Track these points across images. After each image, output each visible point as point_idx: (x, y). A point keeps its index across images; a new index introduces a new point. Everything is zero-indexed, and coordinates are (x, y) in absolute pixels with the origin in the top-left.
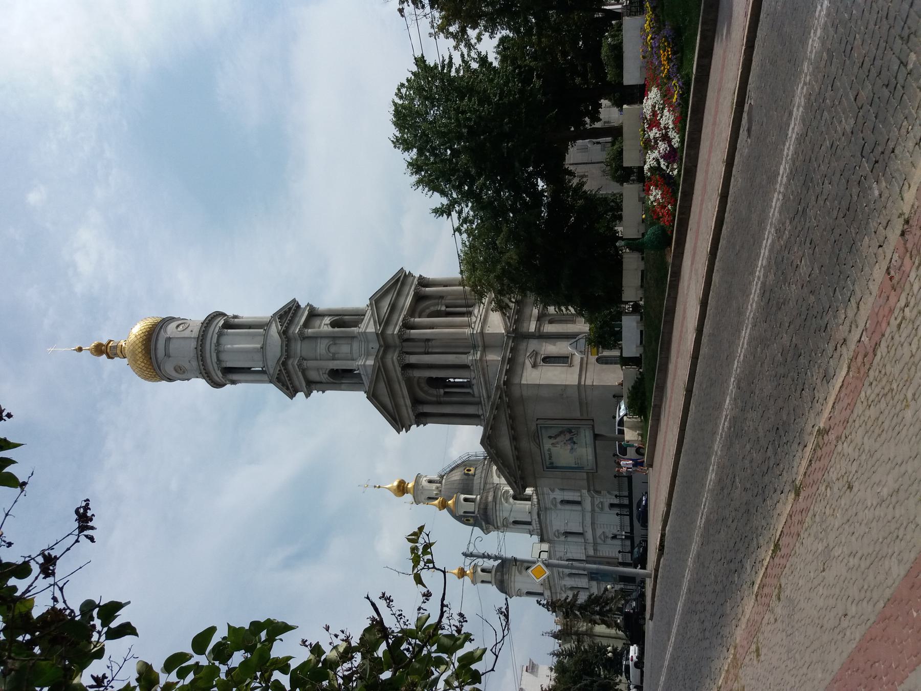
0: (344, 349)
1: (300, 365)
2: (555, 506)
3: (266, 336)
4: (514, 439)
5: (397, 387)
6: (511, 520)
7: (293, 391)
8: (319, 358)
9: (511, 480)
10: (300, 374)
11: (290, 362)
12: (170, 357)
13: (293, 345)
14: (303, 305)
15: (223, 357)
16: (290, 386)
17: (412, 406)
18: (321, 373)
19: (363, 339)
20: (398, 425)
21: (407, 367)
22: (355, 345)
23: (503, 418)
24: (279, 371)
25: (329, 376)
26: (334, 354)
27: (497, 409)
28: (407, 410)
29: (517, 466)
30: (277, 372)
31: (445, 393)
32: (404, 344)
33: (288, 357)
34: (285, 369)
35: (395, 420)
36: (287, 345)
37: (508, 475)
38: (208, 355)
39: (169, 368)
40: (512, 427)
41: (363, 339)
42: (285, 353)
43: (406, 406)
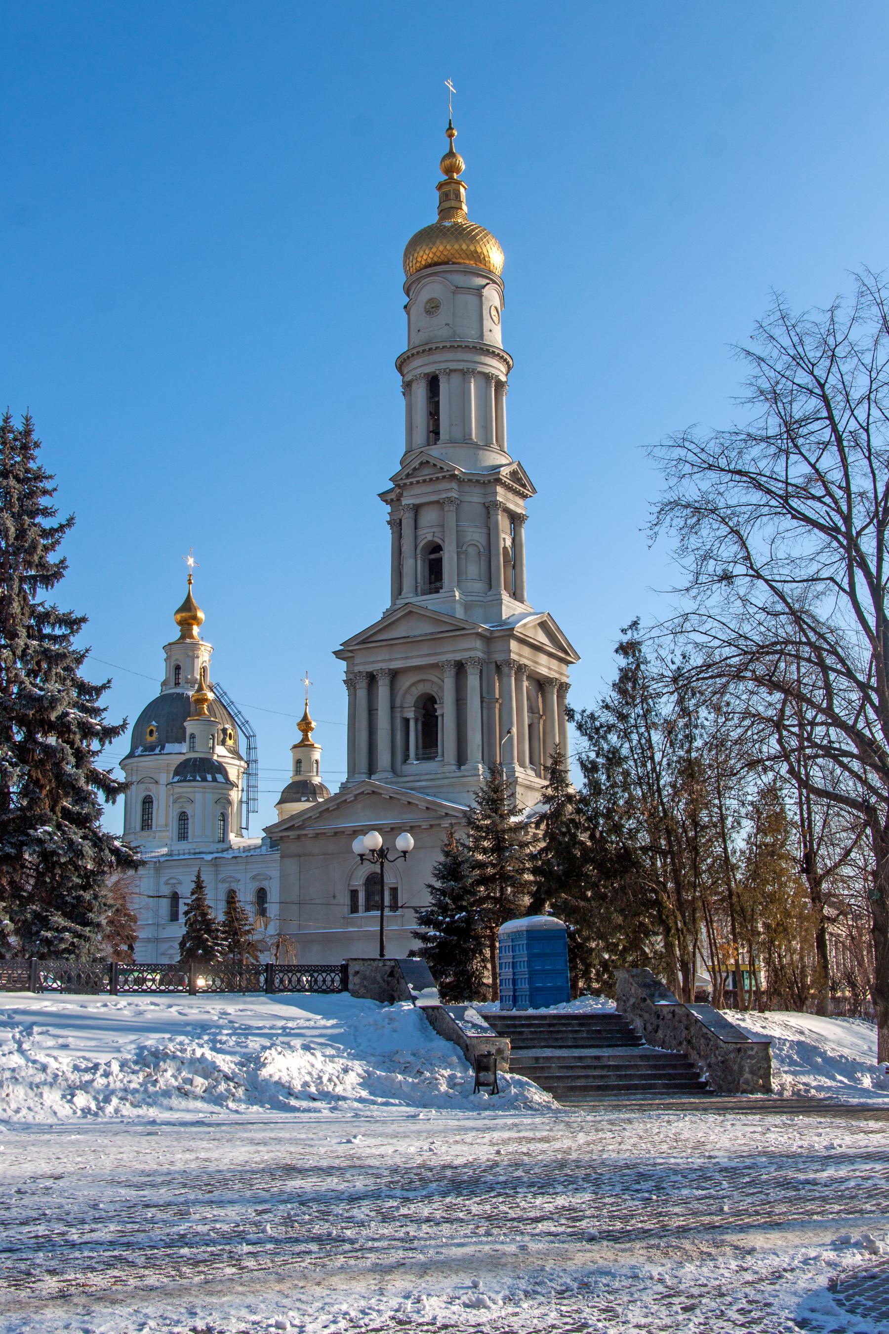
0: (473, 570)
1: (450, 500)
2: (224, 881)
5: (425, 649)
6: (189, 810)
7: (405, 484)
8: (460, 529)
9: (296, 821)
10: (435, 498)
11: (454, 485)
12: (454, 293)
13: (478, 490)
15: (456, 379)
16: (414, 480)
17: (390, 670)
21: (460, 668)
22: (479, 586)
24: (442, 468)
25: (429, 541)
26: (466, 553)
30: (439, 465)
31: (407, 721)
32: (493, 666)
34: (444, 477)
35: (364, 642)
36: (478, 481)
37: (306, 817)
39: (433, 289)
43: (391, 660)
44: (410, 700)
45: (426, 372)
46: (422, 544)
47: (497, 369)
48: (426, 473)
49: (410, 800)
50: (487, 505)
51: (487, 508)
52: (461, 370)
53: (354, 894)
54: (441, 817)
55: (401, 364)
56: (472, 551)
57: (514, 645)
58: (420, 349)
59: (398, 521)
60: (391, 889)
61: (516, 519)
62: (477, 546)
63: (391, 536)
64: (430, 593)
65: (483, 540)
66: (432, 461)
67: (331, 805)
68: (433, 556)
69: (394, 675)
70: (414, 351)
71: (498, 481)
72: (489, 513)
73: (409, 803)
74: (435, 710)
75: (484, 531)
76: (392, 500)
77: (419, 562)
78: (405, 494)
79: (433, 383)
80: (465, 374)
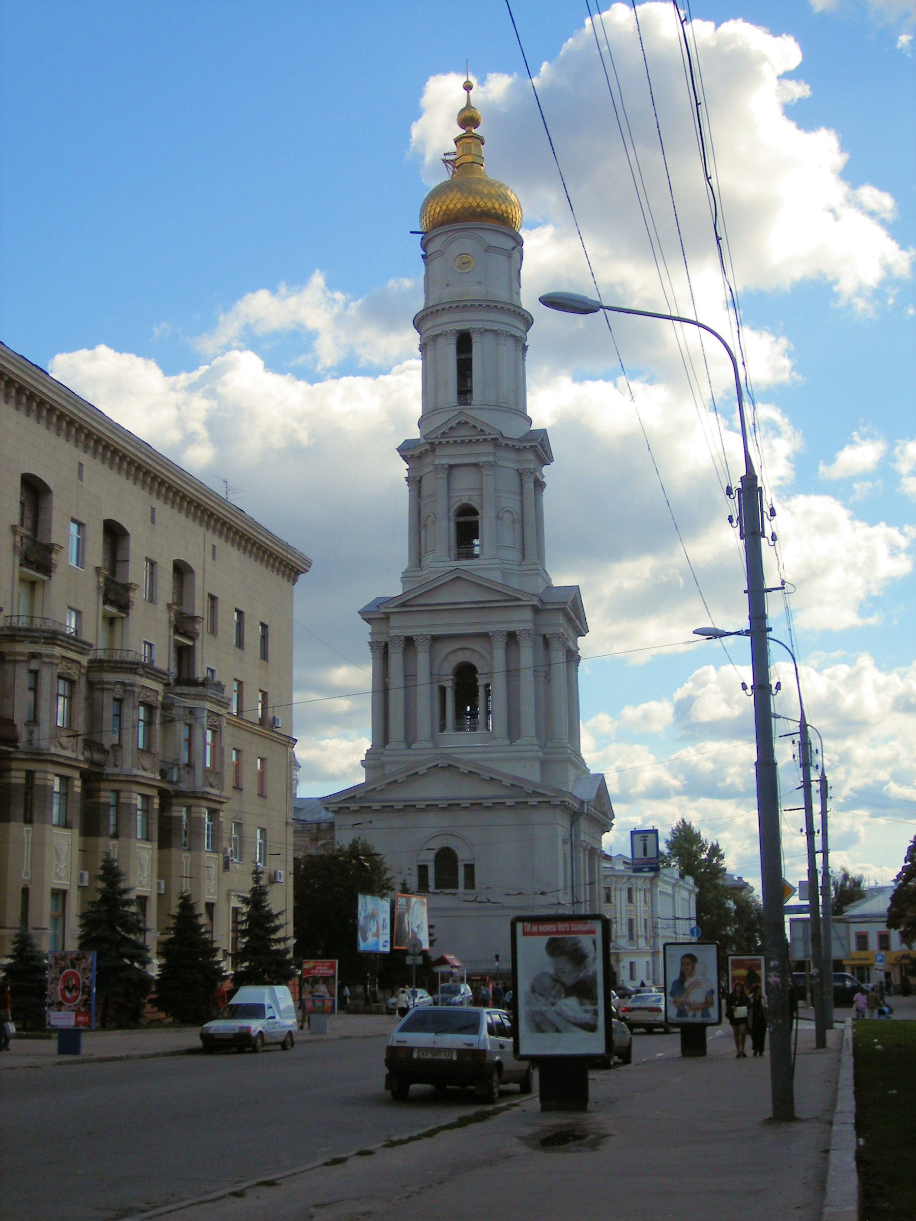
0: (509, 537)
4: (452, 806)
5: (472, 617)
7: (440, 443)
12: (486, 251)
13: (512, 455)
14: (545, 469)
15: (489, 339)
18: (470, 493)
19: (524, 568)
20: (396, 607)
22: (515, 555)
23: (486, 791)
24: (482, 430)
25: (466, 505)
27: (512, 785)
28: (426, 626)
29: (392, 804)
34: (485, 440)
38: (493, 316)
40: (476, 805)
41: (524, 568)
43: (433, 626)
44: (448, 669)
45: (458, 328)
46: (456, 506)
48: (463, 433)
49: (493, 776)
50: (520, 471)
51: (520, 475)
53: (423, 869)
54: (530, 795)
56: (507, 517)
57: (561, 620)
59: (418, 479)
60: (466, 866)
62: (511, 513)
65: (517, 509)
66: (472, 422)
67: (400, 776)
68: (462, 519)
69: (436, 639)
70: (446, 306)
72: (521, 480)
73: (491, 779)
74: (476, 680)
75: (519, 498)
76: (412, 456)
78: (438, 452)
79: (464, 342)
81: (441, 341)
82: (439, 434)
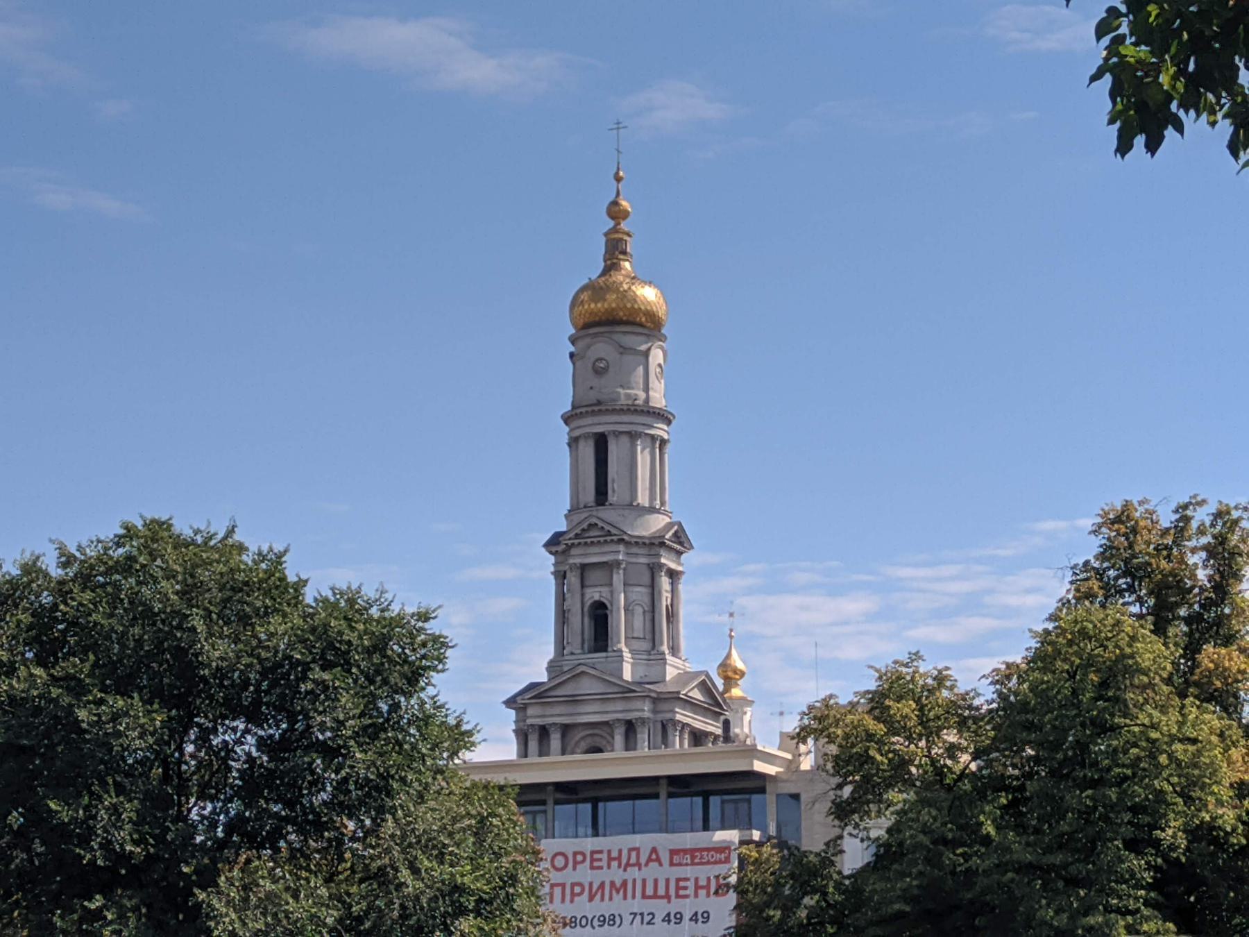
3: (652, 510)
11: (621, 548)
16: (582, 541)
33: (627, 544)
39: (602, 349)
41: (652, 657)
42: (633, 540)
47: (660, 430)
52: (629, 433)
55: (567, 419)
58: (589, 409)
61: (673, 575)
63: (553, 581)
64: (596, 650)
65: (647, 599)
71: (662, 544)
77: (586, 620)
78: (574, 551)
79: (601, 443)
80: (633, 436)
81: (582, 444)
82: (572, 535)
